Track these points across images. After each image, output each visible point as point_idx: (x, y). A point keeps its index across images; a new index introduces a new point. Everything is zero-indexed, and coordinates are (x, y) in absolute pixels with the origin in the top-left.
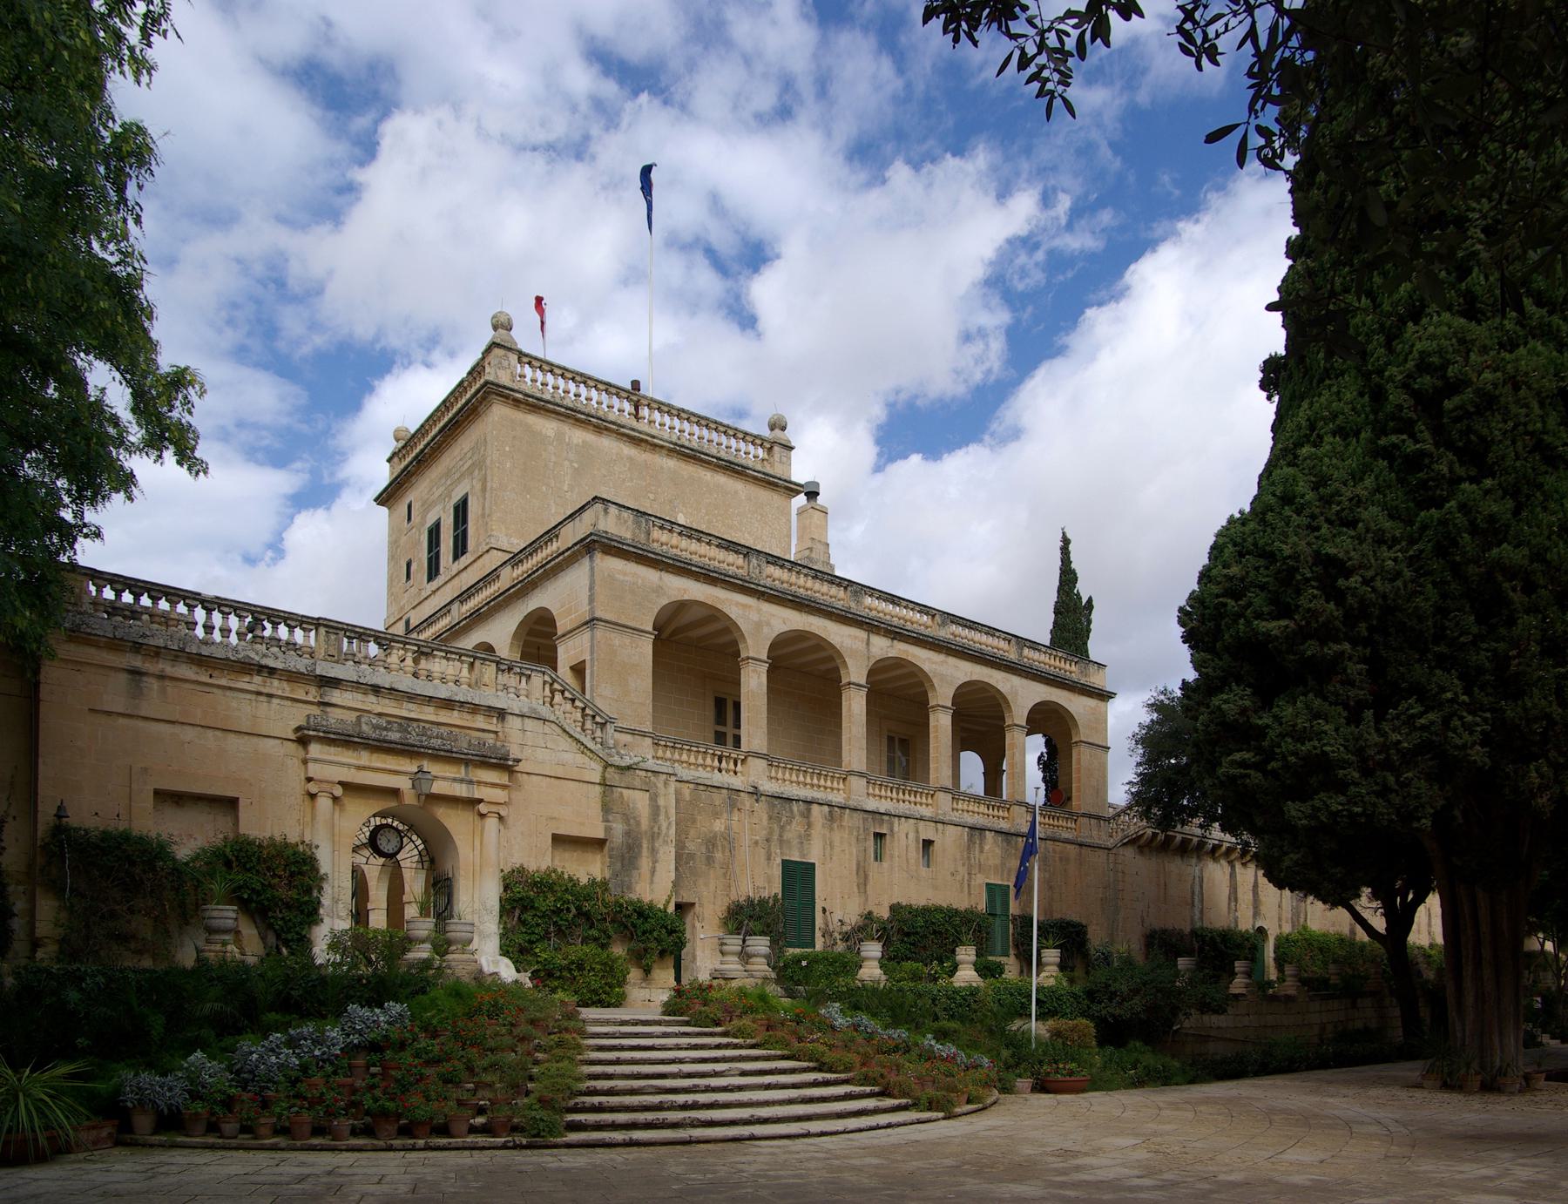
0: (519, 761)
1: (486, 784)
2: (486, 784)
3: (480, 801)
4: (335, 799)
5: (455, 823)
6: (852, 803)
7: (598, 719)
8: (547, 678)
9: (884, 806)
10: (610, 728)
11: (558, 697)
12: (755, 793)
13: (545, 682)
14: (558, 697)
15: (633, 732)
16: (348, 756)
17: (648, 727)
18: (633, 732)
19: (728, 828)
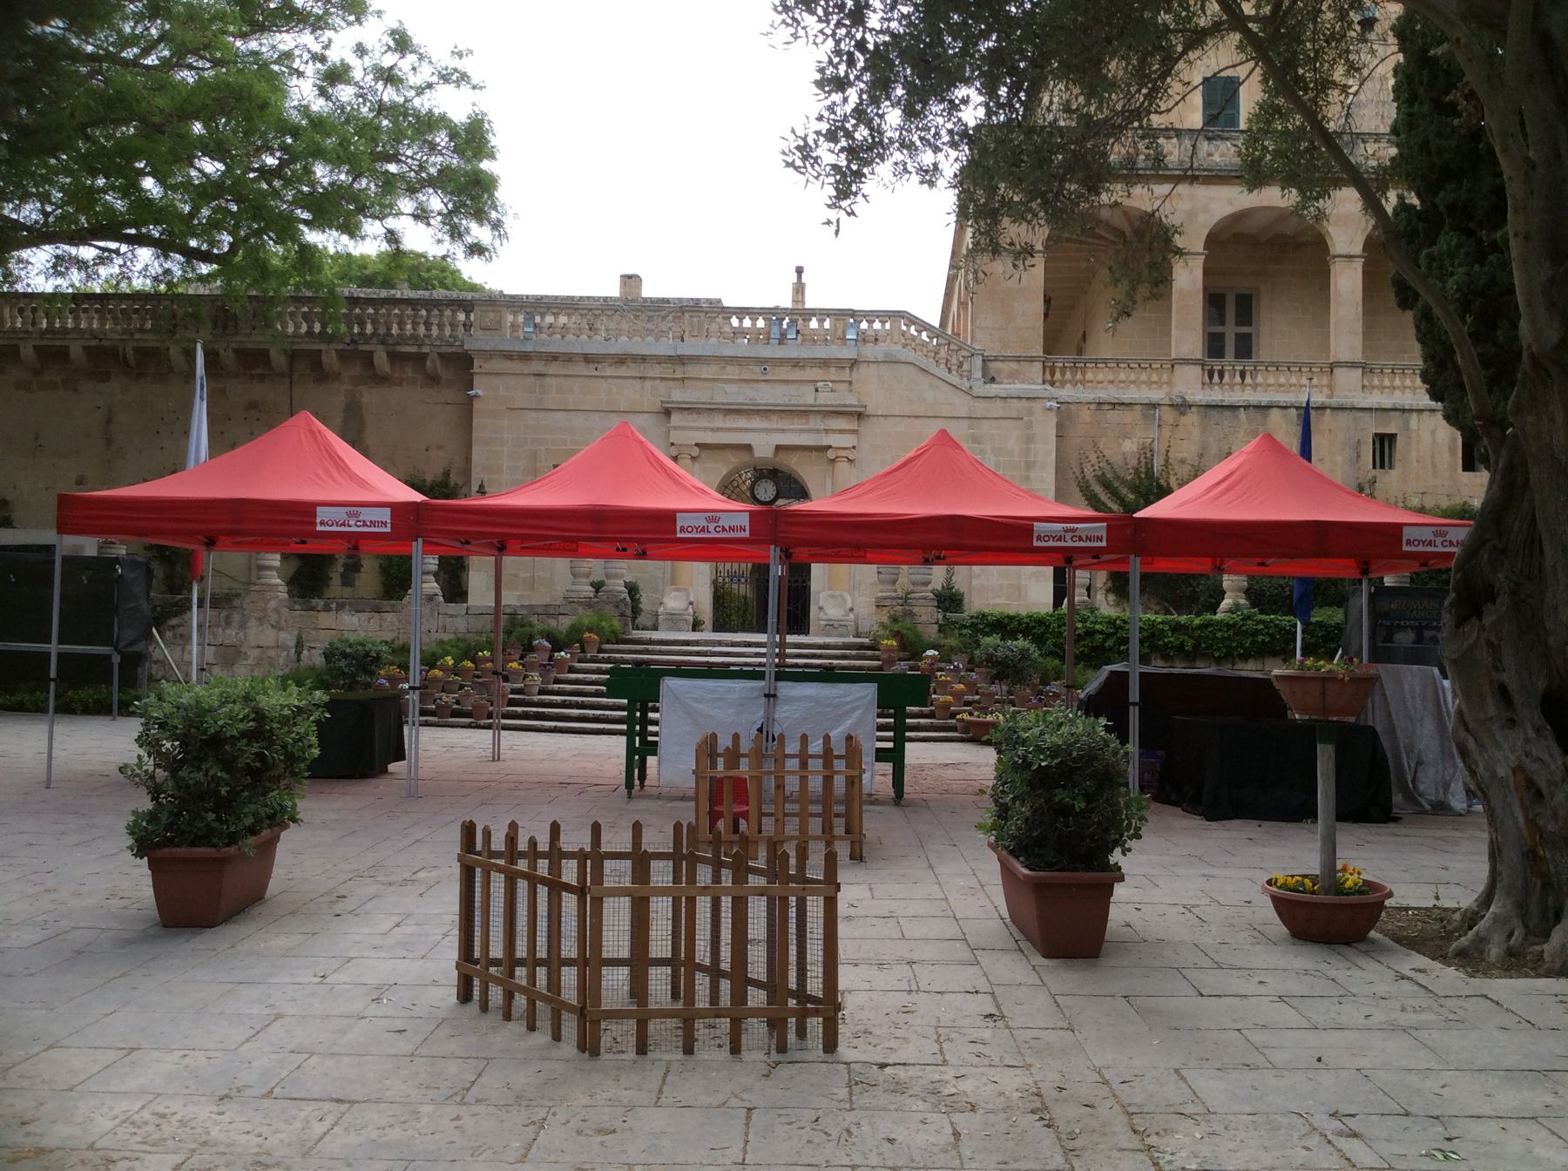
1: (834, 431)
2: (834, 431)
4: (693, 458)
5: (809, 472)
6: (1334, 401)
9: (1387, 401)
12: (1182, 407)
15: (1018, 359)
16: (703, 421)
18: (1018, 359)
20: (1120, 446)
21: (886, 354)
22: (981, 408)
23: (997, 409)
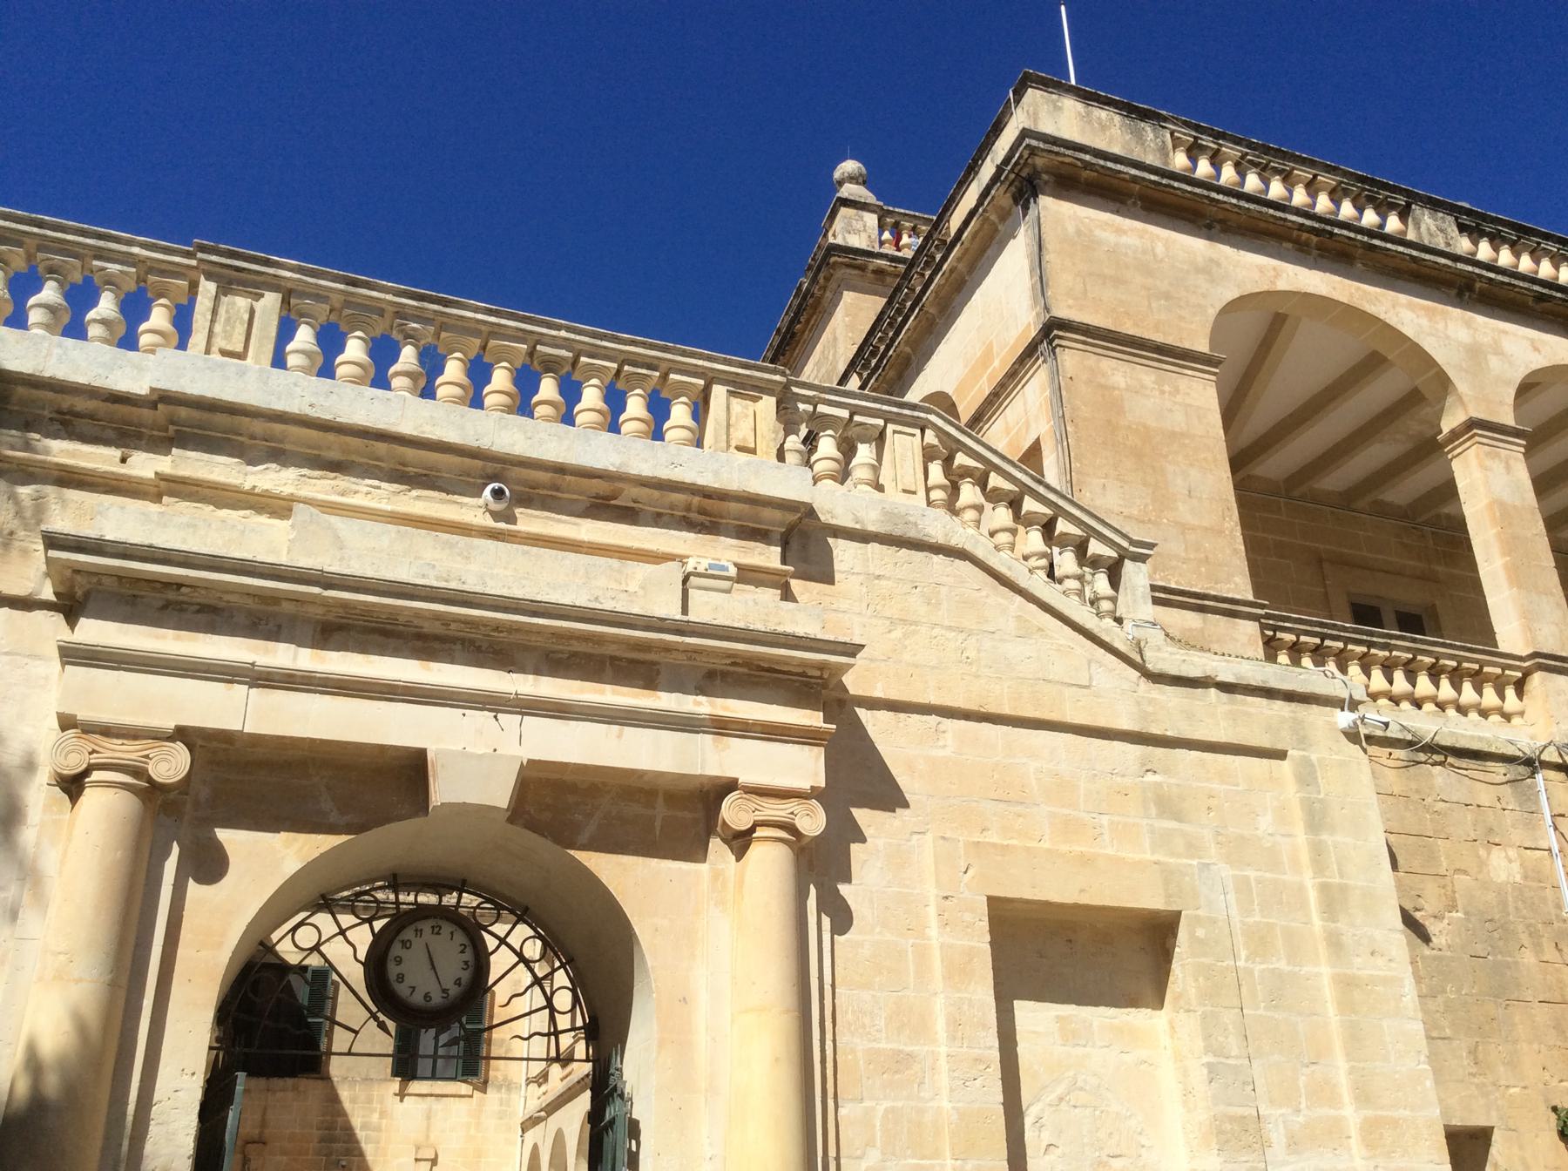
0: (852, 650)
3: (730, 786)
7: (1095, 547)
8: (931, 437)
10: (1136, 576)
11: (969, 493)
13: (929, 455)
14: (969, 493)
17: (1240, 586)
19: (1535, 876)
20: (1482, 864)
21: (888, 515)
22: (1172, 711)
23: (1212, 716)
